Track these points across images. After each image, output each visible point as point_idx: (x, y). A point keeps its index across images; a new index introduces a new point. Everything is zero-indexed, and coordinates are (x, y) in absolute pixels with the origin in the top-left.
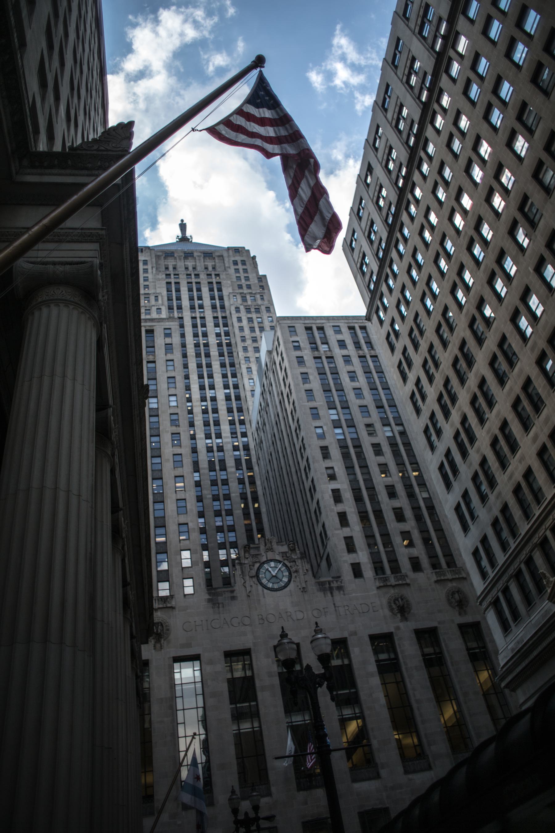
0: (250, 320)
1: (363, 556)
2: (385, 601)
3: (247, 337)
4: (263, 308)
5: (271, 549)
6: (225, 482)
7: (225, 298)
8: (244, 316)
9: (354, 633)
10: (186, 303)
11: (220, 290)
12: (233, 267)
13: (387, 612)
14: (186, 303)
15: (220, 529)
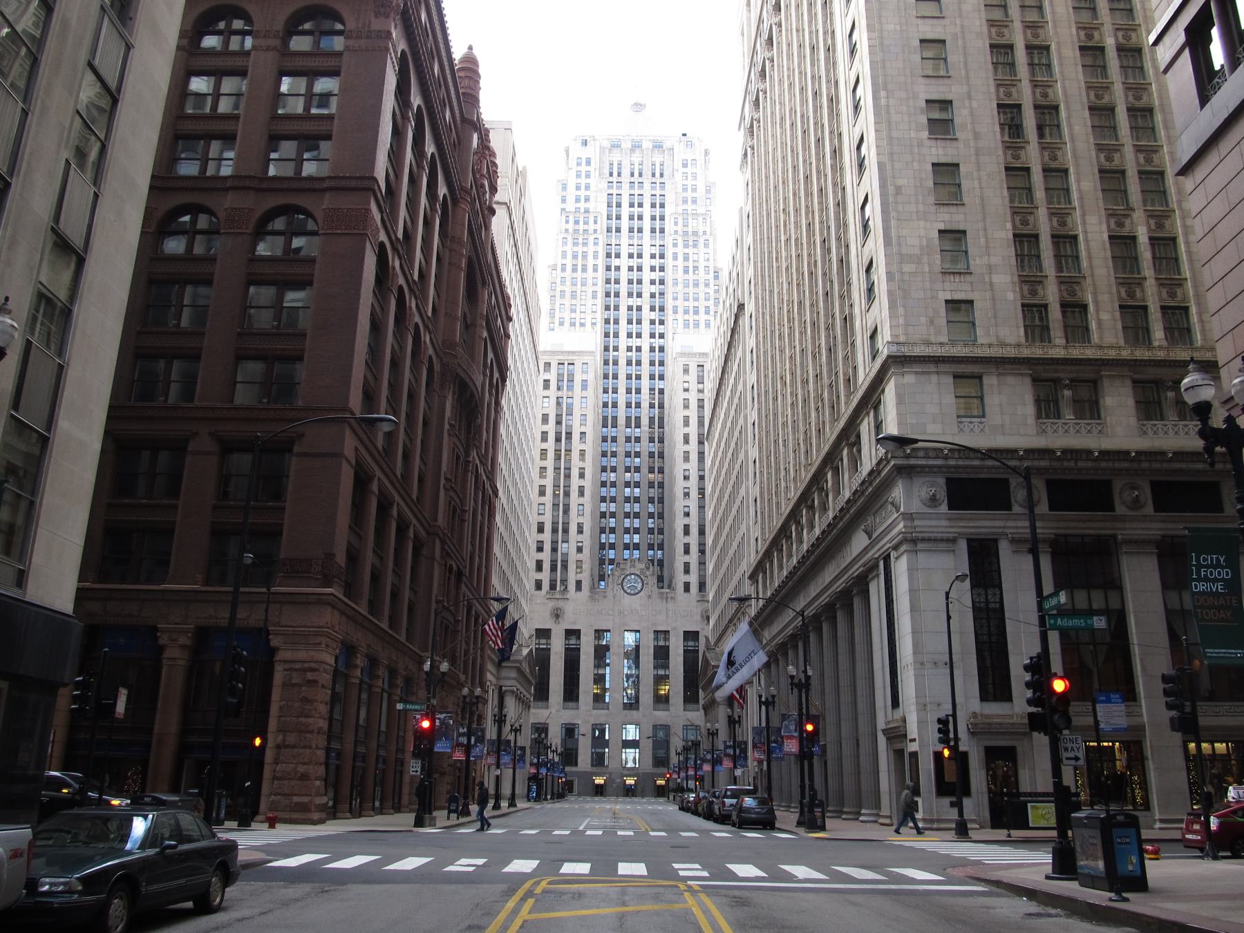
0: (686, 258)
1: (693, 579)
2: (699, 611)
3: (680, 280)
4: (701, 241)
5: (634, 566)
6: (638, 440)
7: (667, 218)
8: (680, 250)
9: (675, 629)
10: (625, 224)
11: (662, 206)
12: (682, 170)
13: (699, 617)
14: (625, 224)
15: (627, 484)
